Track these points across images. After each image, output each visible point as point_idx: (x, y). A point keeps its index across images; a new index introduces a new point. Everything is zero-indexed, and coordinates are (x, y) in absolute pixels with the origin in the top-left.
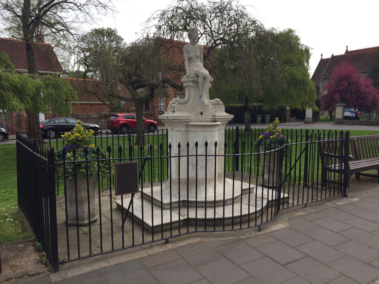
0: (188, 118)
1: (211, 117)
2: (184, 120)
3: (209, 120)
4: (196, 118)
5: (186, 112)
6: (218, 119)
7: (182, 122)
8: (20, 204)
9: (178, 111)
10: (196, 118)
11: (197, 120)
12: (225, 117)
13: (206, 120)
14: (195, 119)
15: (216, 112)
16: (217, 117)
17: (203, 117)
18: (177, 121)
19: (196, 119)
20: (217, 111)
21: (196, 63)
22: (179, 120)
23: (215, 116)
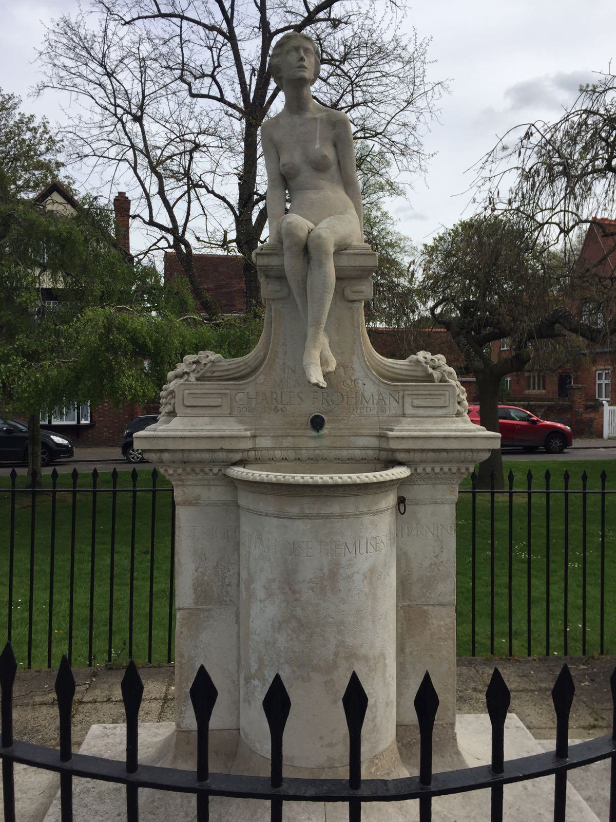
0: (227, 445)
1: (374, 442)
2: (206, 456)
3: (358, 453)
4: (286, 443)
5: (231, 415)
6: (408, 451)
7: (200, 462)
8: (142, 688)
9: (189, 411)
10: (286, 443)
11: (291, 454)
12: (171, 446)
13: (345, 453)
14: (280, 449)
15: (404, 415)
16: (393, 445)
17: (326, 442)
18: (166, 456)
19: (288, 448)
20: (409, 410)
21: (312, 195)
22: (179, 456)
23: (387, 438)
